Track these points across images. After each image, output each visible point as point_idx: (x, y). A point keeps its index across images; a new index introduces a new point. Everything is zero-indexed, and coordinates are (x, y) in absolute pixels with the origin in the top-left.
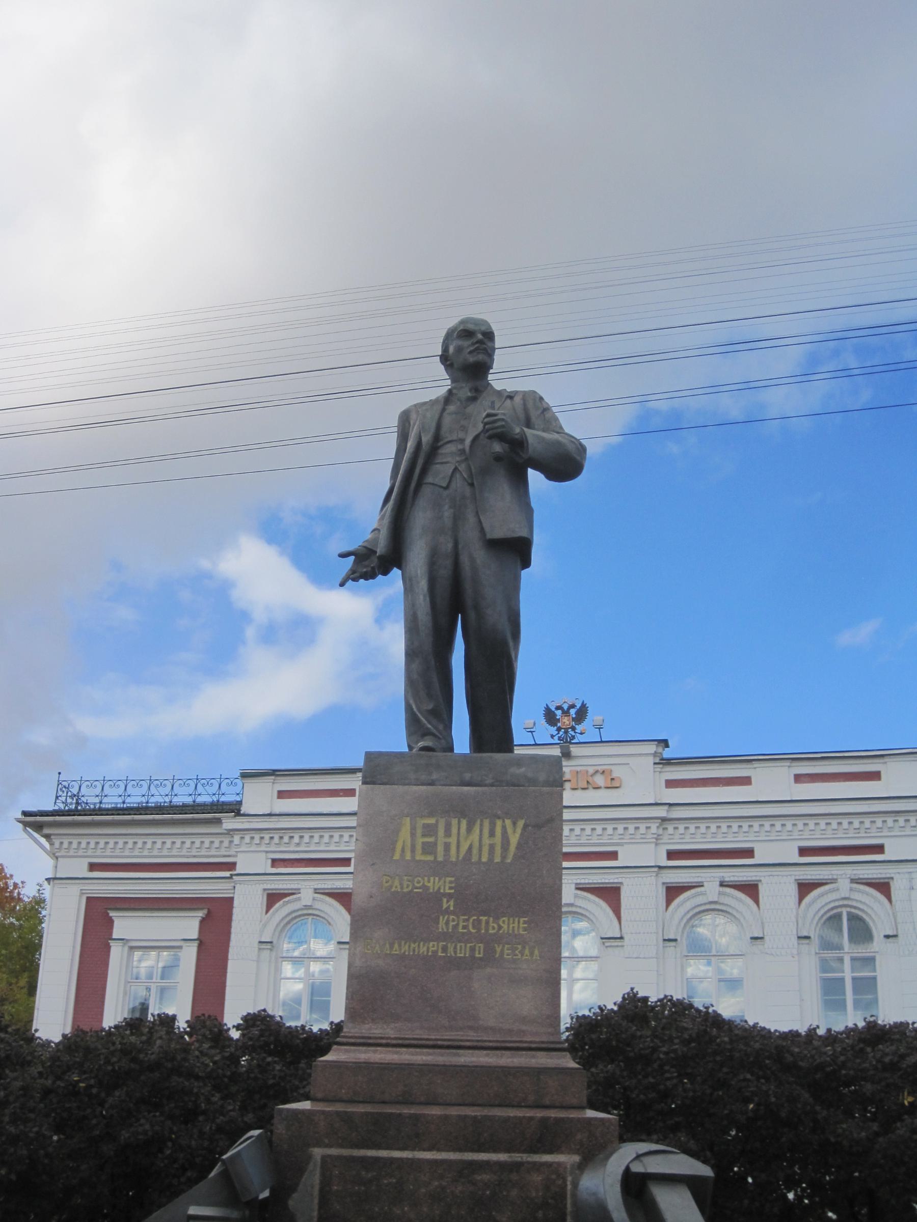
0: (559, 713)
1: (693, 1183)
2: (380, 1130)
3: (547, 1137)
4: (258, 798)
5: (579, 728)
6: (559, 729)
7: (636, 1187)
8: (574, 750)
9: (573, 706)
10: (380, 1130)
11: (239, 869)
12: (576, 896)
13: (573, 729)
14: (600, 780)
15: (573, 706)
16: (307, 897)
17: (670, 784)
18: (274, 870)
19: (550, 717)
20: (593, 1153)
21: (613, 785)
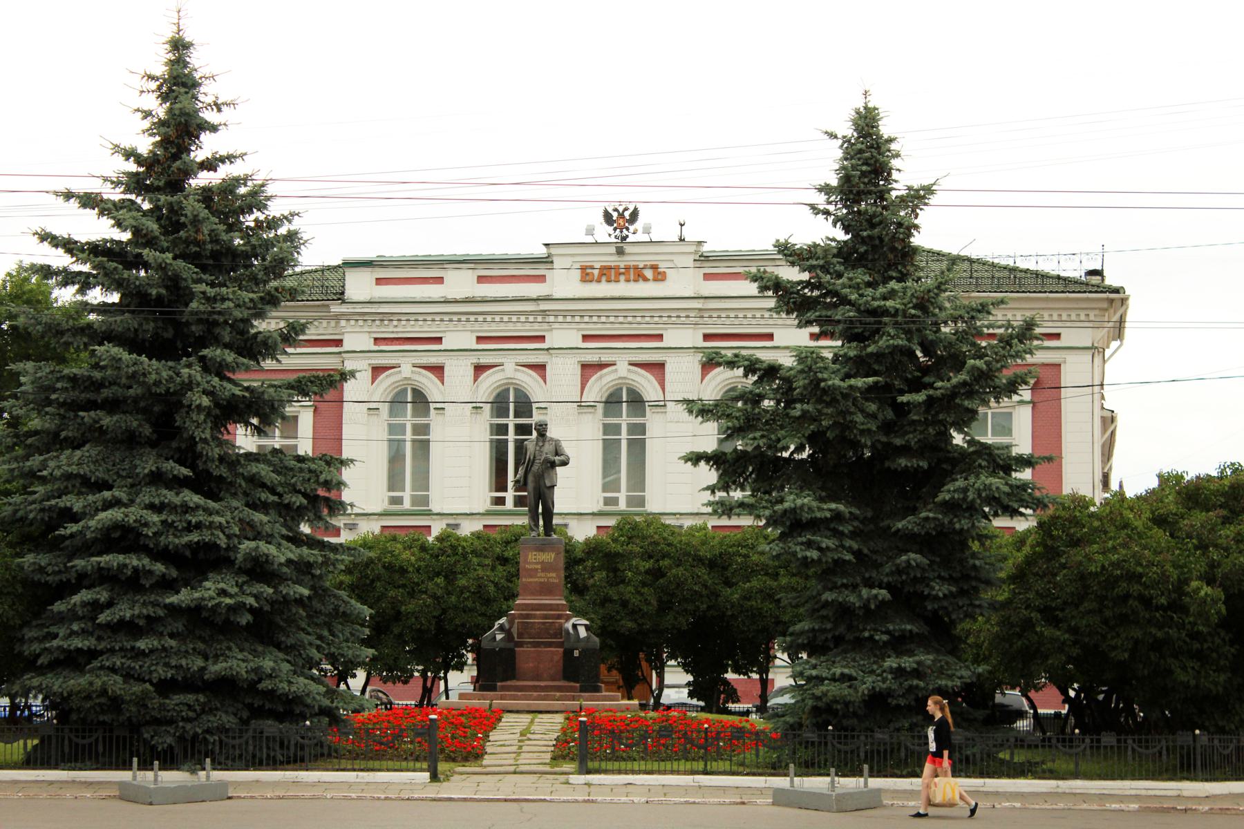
0: (615, 215)
1: (586, 626)
2: (528, 616)
3: (559, 617)
4: (359, 286)
5: (632, 228)
6: (615, 229)
7: (575, 626)
8: (628, 249)
9: (626, 209)
10: (528, 616)
11: (347, 346)
12: (629, 371)
13: (628, 229)
14: (649, 274)
15: (626, 209)
16: (406, 370)
17: (707, 277)
18: (376, 348)
19: (608, 218)
20: (568, 618)
21: (660, 277)
